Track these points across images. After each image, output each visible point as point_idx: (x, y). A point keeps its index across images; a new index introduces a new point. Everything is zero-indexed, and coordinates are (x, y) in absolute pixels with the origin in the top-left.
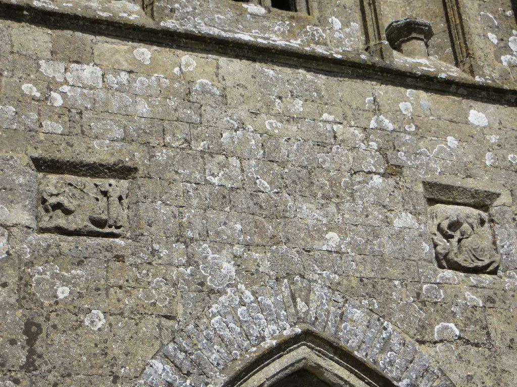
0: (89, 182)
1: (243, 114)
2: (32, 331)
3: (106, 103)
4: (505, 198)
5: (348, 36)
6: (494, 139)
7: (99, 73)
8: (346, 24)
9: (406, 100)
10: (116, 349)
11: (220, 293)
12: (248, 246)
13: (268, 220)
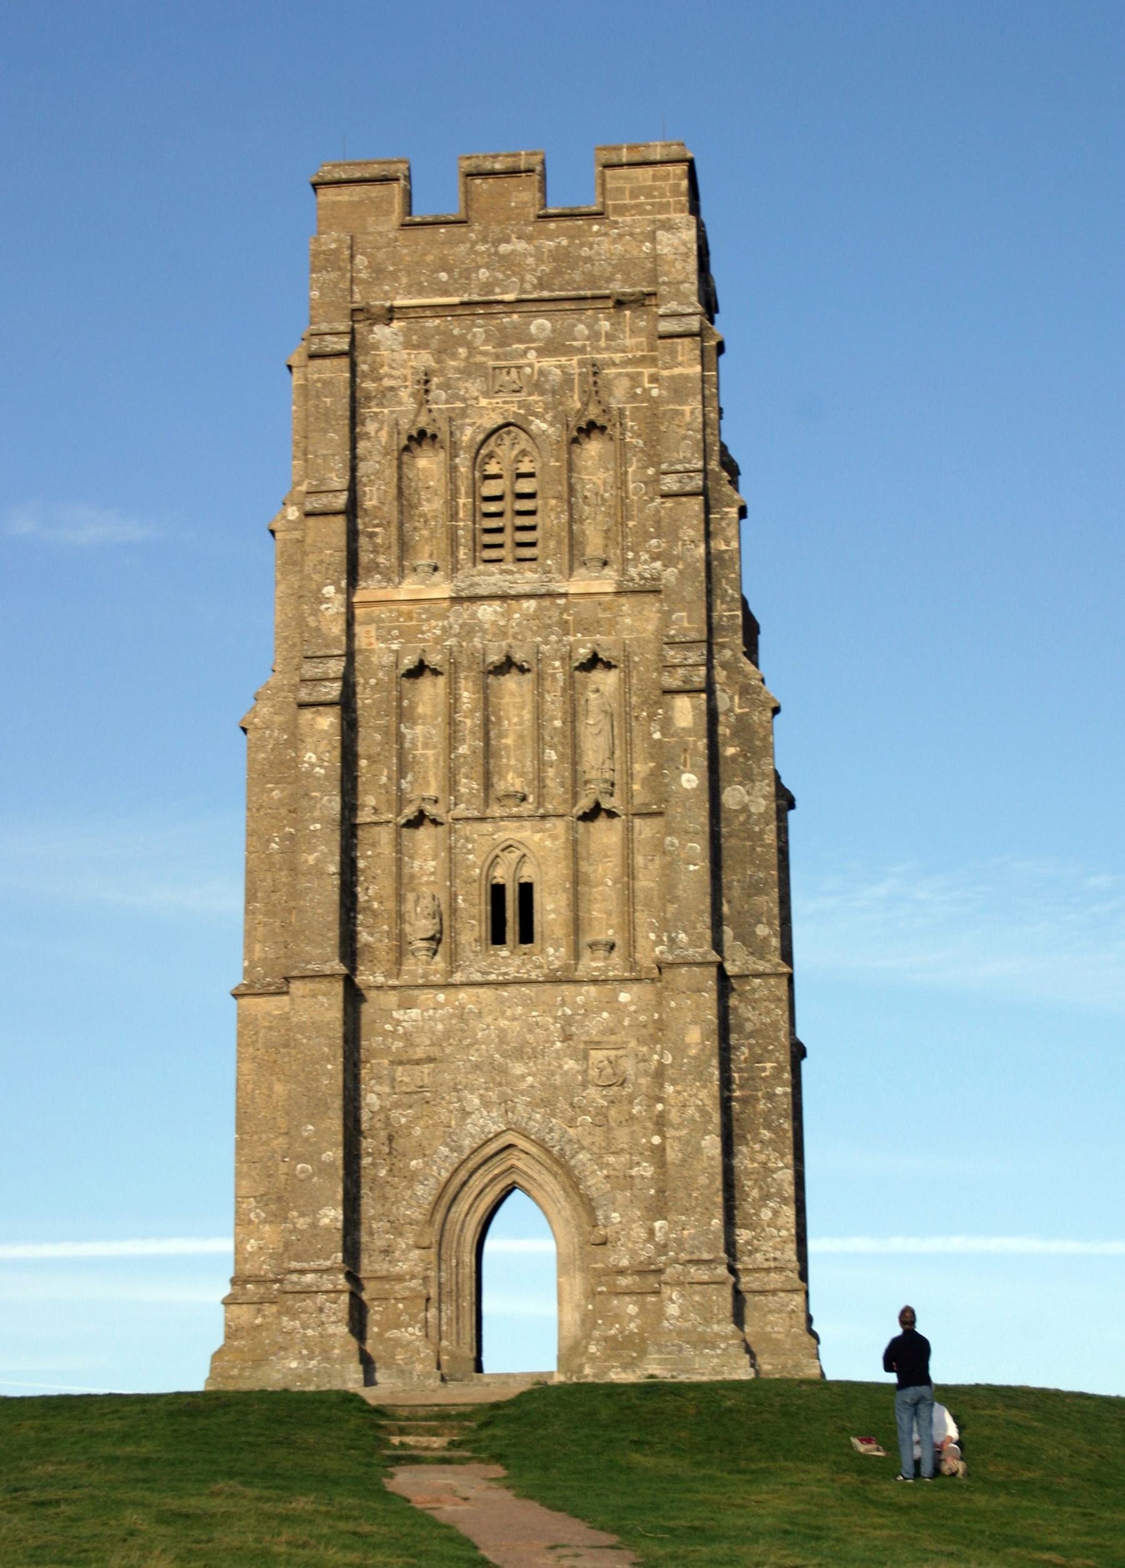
0: (417, 1067)
2: (390, 1138)
3: (423, 1027)
4: (633, 1044)
5: (557, 958)
6: (632, 1008)
7: (419, 1011)
8: (556, 950)
10: (425, 1143)
11: (473, 1113)
12: (486, 1089)
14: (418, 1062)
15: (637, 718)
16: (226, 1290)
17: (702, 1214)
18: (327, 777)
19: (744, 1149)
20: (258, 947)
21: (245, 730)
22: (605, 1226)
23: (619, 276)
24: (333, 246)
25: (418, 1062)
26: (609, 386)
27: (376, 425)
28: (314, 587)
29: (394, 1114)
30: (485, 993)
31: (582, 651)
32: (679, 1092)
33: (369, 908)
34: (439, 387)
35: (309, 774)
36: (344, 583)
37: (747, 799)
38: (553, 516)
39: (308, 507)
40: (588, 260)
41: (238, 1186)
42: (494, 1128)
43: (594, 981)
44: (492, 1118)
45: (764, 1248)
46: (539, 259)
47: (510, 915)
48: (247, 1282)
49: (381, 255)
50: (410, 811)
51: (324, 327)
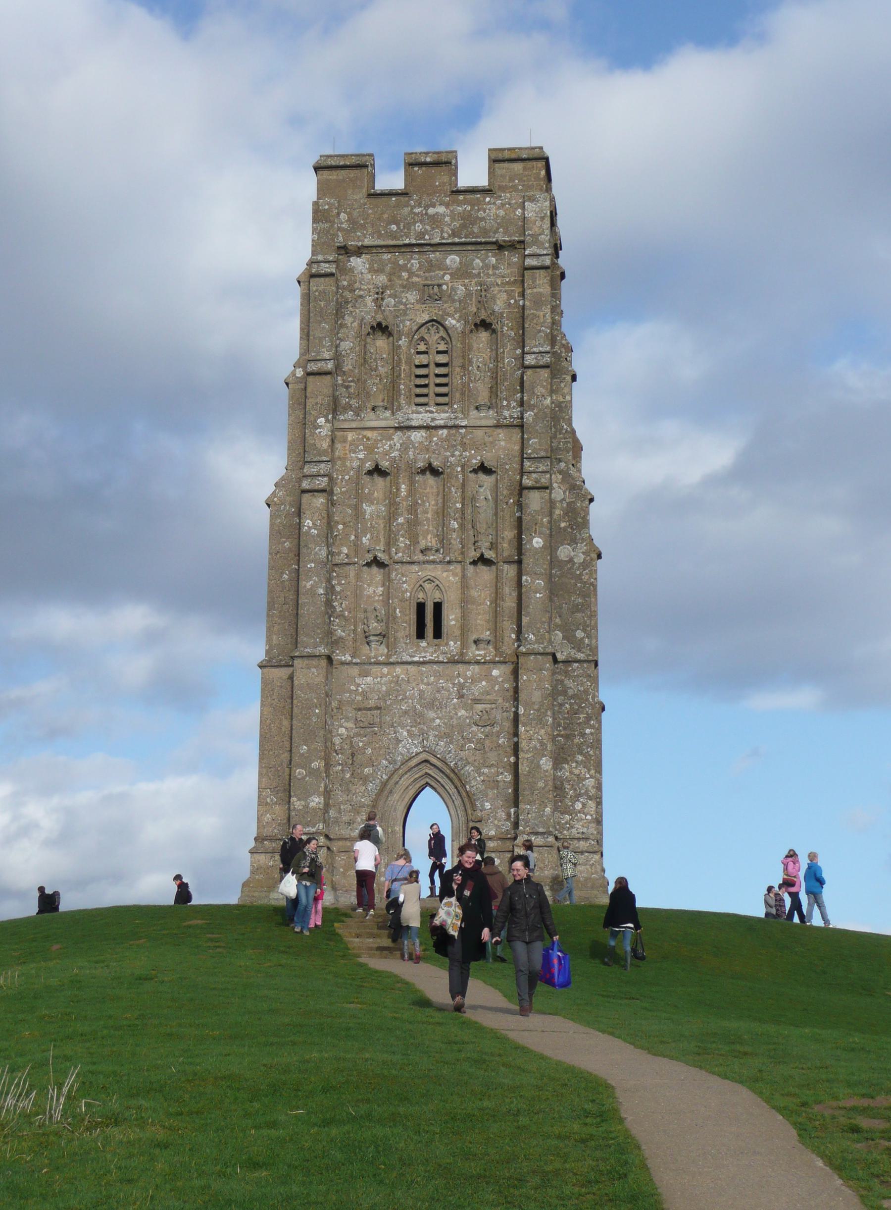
0: (369, 712)
1: (414, 685)
2: (353, 755)
4: (501, 701)
6: (500, 680)
9: (469, 670)
13: (418, 718)
14: (370, 709)
15: (507, 503)
16: (252, 844)
17: (540, 805)
18: (318, 535)
19: (566, 766)
20: (275, 637)
21: (269, 505)
22: (481, 811)
23: (501, 230)
24: (327, 207)
25: (370, 709)
26: (494, 298)
27: (351, 319)
28: (312, 419)
29: (355, 740)
30: (412, 669)
31: (474, 461)
32: (528, 731)
33: (343, 616)
34: (390, 296)
35: (308, 533)
36: (330, 417)
37: (572, 554)
38: (458, 377)
39: (309, 370)
40: (483, 219)
41: (260, 782)
42: (415, 750)
43: (478, 663)
44: (414, 744)
45: (577, 826)
46: (453, 219)
47: (428, 621)
48: (264, 839)
49: (355, 214)
50: (369, 557)
51: (320, 258)
